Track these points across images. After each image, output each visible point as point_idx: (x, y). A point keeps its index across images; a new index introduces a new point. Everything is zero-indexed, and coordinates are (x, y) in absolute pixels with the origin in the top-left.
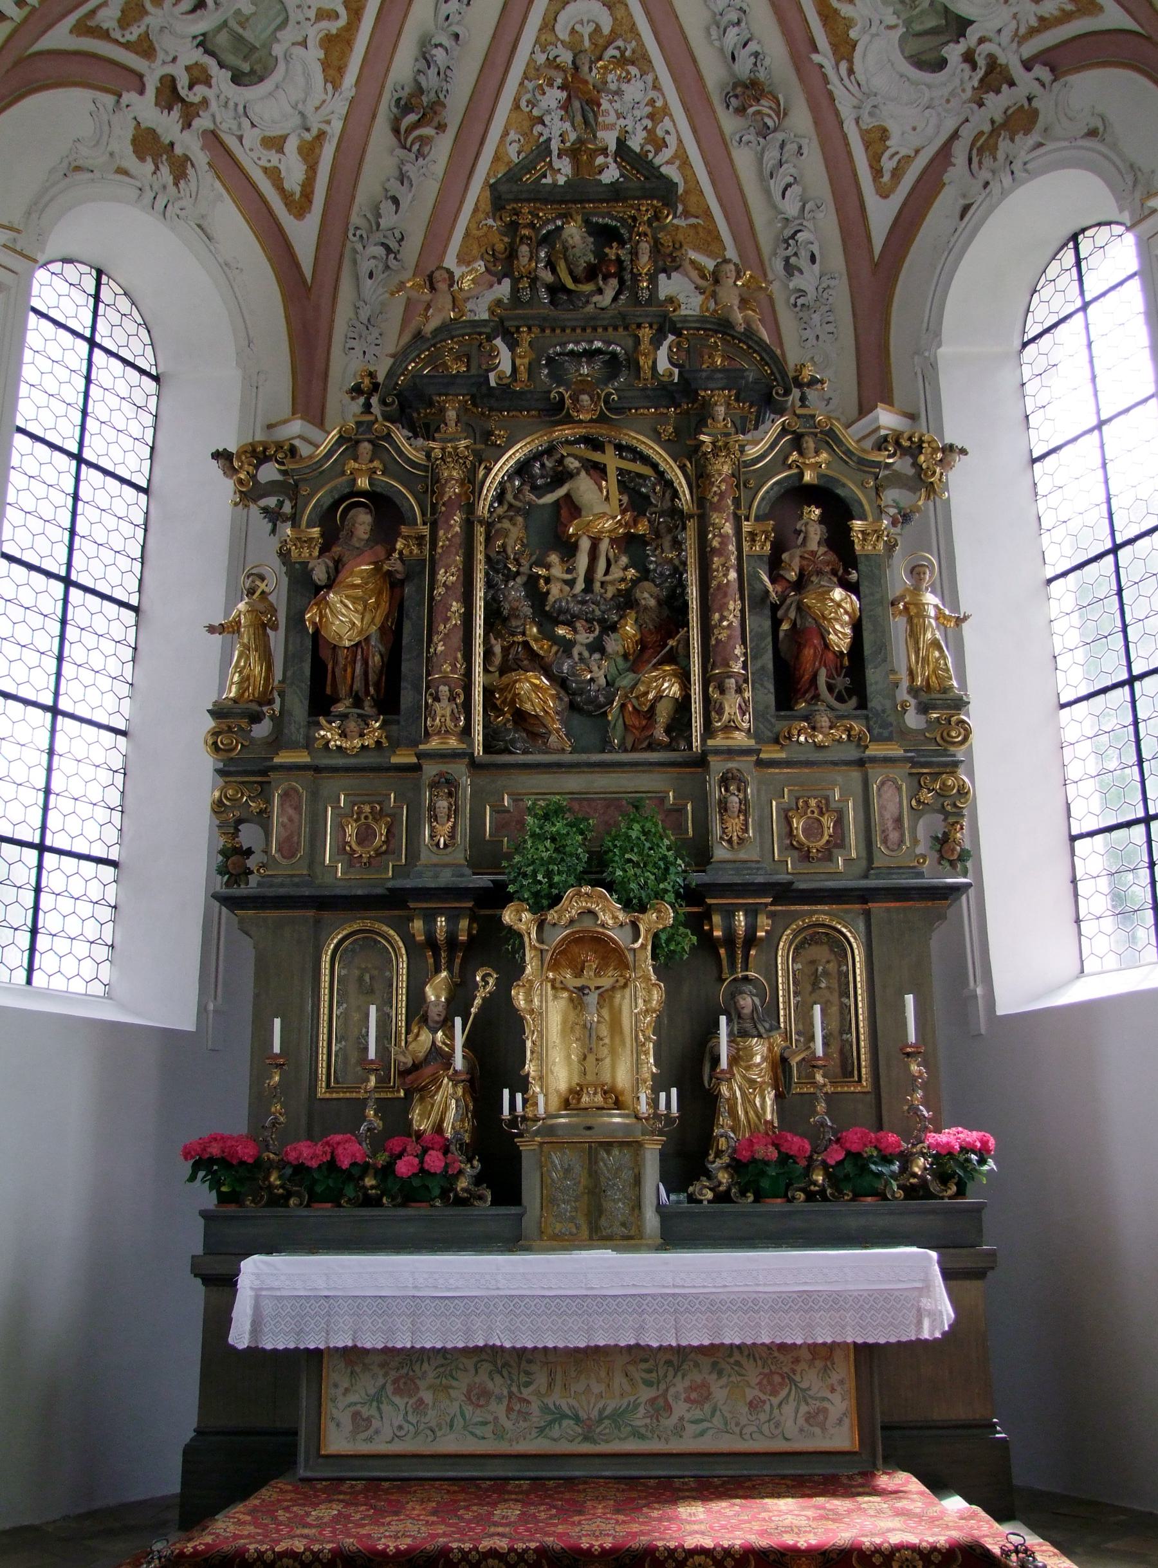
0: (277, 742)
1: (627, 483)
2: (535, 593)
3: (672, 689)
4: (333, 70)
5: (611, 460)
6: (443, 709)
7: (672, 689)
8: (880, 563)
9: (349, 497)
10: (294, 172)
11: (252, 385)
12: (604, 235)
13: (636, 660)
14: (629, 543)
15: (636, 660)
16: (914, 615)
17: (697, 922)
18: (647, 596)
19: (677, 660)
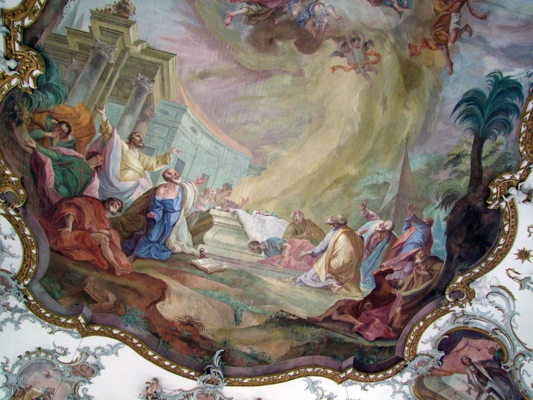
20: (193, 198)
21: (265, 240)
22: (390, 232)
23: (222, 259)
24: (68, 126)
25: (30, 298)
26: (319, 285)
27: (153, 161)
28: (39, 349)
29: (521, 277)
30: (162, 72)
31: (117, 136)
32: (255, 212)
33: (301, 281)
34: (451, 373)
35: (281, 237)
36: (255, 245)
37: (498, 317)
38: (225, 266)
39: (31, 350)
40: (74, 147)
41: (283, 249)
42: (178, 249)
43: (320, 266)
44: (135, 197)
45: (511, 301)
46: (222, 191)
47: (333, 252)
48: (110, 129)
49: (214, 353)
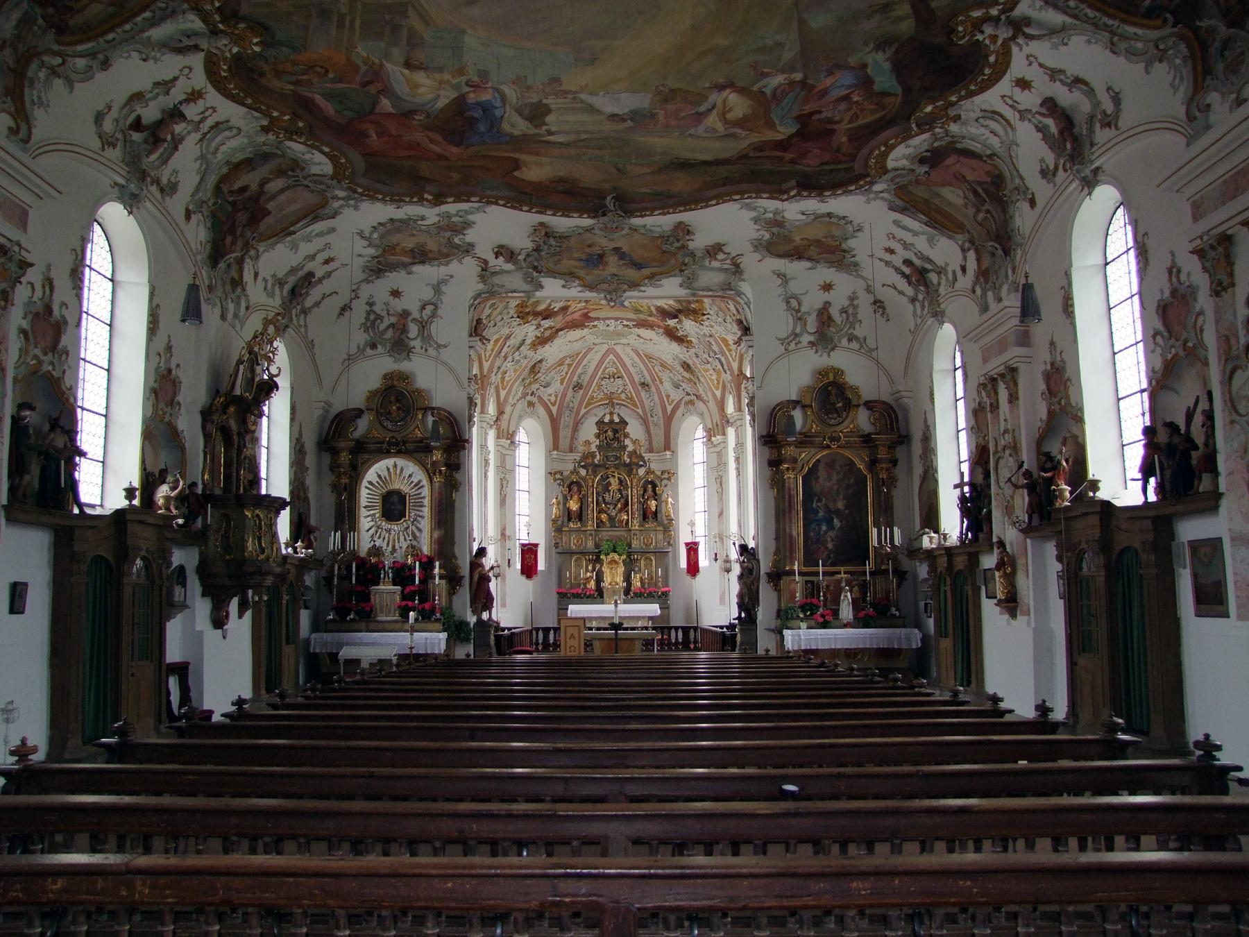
0: (563, 525)
1: (619, 478)
2: (604, 500)
3: (626, 517)
4: (562, 383)
5: (616, 474)
6: (590, 522)
7: (626, 517)
8: (661, 495)
9: (572, 483)
10: (553, 399)
11: (546, 445)
12: (615, 431)
13: (621, 511)
14: (619, 490)
15: (621, 511)
16: (667, 503)
17: (629, 556)
18: (622, 501)
19: (627, 512)
20: (514, 95)
21: (626, 111)
22: (803, 83)
23: (578, 132)
24: (322, 67)
25: (360, 190)
26: (718, 135)
27: (447, 76)
28: (391, 219)
29: (1021, 107)
30: (414, 8)
31: (389, 66)
32: (601, 93)
33: (690, 135)
34: (944, 185)
35: (647, 106)
36: (614, 117)
37: (995, 142)
38: (584, 136)
39: (383, 220)
40: (340, 81)
41: (653, 116)
42: (516, 133)
43: (713, 120)
44: (440, 104)
45: (1009, 129)
46: (550, 84)
47: (725, 106)
48: (377, 61)
49: (605, 198)
